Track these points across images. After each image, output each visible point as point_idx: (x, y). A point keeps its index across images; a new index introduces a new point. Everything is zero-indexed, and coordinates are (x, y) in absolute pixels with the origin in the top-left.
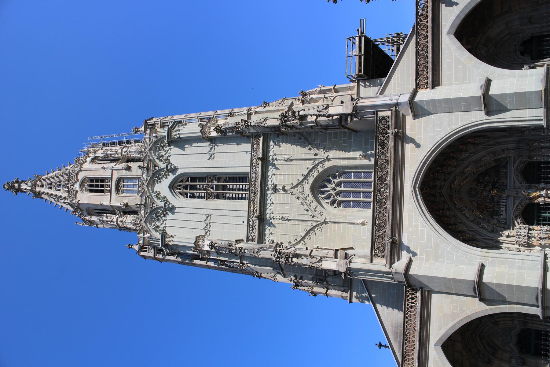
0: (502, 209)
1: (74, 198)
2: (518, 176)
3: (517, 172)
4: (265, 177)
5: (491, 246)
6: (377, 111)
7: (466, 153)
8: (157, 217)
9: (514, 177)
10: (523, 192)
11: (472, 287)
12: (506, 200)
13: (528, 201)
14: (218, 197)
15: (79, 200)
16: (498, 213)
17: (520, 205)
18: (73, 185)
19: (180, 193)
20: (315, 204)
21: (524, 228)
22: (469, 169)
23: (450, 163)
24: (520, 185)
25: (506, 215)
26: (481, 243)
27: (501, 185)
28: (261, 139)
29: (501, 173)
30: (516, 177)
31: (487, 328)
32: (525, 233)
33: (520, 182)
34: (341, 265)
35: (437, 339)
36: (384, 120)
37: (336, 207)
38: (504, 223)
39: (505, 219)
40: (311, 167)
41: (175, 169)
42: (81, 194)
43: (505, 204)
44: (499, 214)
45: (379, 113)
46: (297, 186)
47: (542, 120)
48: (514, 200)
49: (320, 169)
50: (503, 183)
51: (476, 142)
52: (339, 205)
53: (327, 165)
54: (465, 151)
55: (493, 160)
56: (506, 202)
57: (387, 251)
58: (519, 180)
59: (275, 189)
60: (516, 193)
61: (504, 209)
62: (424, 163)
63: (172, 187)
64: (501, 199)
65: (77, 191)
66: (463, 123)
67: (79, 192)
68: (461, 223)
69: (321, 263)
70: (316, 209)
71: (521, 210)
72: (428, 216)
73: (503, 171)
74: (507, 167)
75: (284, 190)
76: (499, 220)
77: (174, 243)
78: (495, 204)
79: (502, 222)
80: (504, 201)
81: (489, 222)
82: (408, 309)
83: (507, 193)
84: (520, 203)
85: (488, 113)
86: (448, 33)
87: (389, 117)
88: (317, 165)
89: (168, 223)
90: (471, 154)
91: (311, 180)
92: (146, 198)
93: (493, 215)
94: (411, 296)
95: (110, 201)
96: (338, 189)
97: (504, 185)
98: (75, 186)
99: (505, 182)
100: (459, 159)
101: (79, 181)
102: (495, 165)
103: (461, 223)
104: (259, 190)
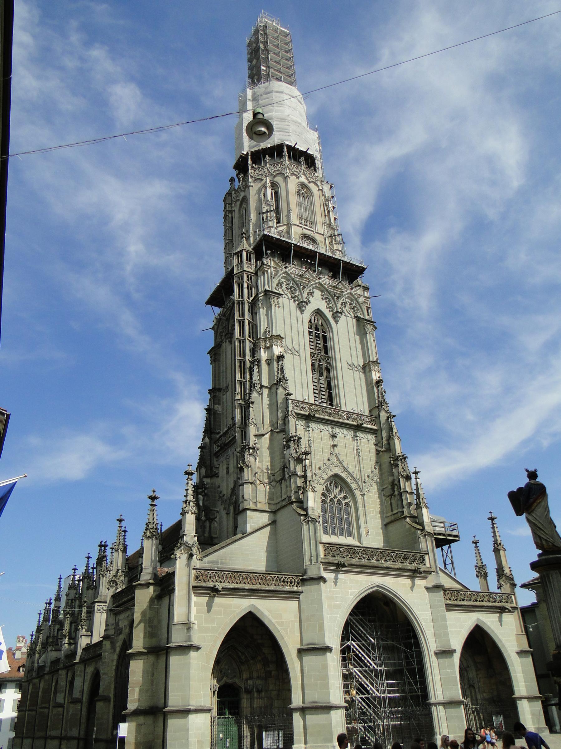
1: (291, 172)
4: (342, 427)
6: (428, 554)
8: (291, 288)
11: (316, 642)
14: (313, 365)
15: (289, 178)
18: (304, 175)
19: (311, 320)
20: (326, 477)
28: (375, 428)
31: (240, 654)
34: (313, 512)
35: (259, 607)
36: (422, 560)
37: (321, 498)
40: (355, 476)
41: (337, 322)
42: (297, 182)
45: (428, 555)
46: (338, 460)
47: (435, 699)
49: (353, 486)
52: (323, 501)
53: (358, 493)
57: (330, 559)
59: (334, 436)
62: (395, 596)
63: (318, 312)
65: (298, 178)
66: (427, 631)
67: (298, 180)
69: (311, 490)
70: (321, 478)
72: (359, 599)
75: (334, 446)
77: (273, 307)
82: (282, 577)
85: (437, 654)
86: (478, 619)
87: (425, 564)
88: (357, 483)
89: (286, 300)
91: (344, 475)
92: (309, 279)
94: (293, 581)
95: (294, 225)
96: (336, 500)
98: (303, 177)
101: (309, 184)
104: (332, 419)
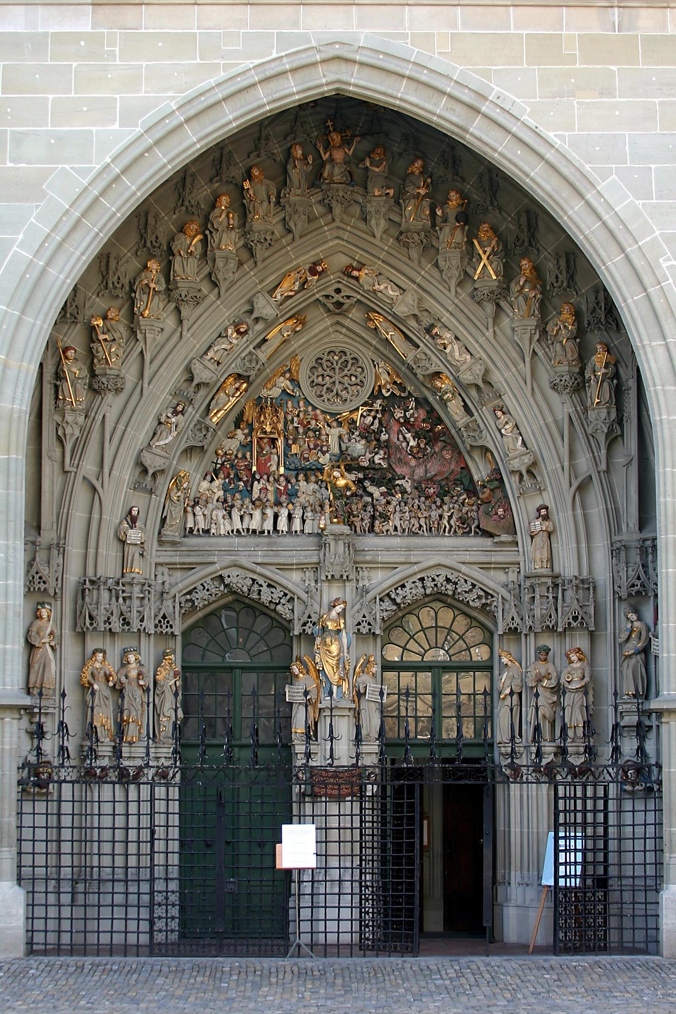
0: (257, 514)
2: (419, 584)
3: (441, 579)
5: (67, 468)
7: (537, 337)
9: (416, 568)
10: (339, 609)
12: (302, 531)
13: (296, 633)
16: (238, 496)
17: (275, 596)
21: (164, 617)
22: (453, 350)
23: (484, 257)
24: (370, 596)
25: (228, 534)
26: (81, 419)
27: (373, 506)
29: (434, 507)
30: (415, 574)
32: (142, 620)
33: (388, 595)
38: (190, 524)
39: (207, 532)
43: (283, 525)
44: (229, 499)
48: (301, 567)
50: (385, 518)
51: (593, 390)
54: (544, 332)
55: (497, 471)
56: (289, 532)
58: (399, 591)
60: (337, 576)
61: (255, 524)
64: (304, 508)
68: (181, 322)
71: (253, 600)
73: (446, 515)
74: (467, 534)
76: (202, 502)
78: (282, 479)
79: (194, 515)
80: (297, 525)
81: (189, 451)
83: (337, 537)
84: (285, 595)
90: (528, 359)
93: (228, 476)
97: (377, 522)
99: (392, 529)
100: (503, 304)
102: (476, 478)
103: (181, 322)
